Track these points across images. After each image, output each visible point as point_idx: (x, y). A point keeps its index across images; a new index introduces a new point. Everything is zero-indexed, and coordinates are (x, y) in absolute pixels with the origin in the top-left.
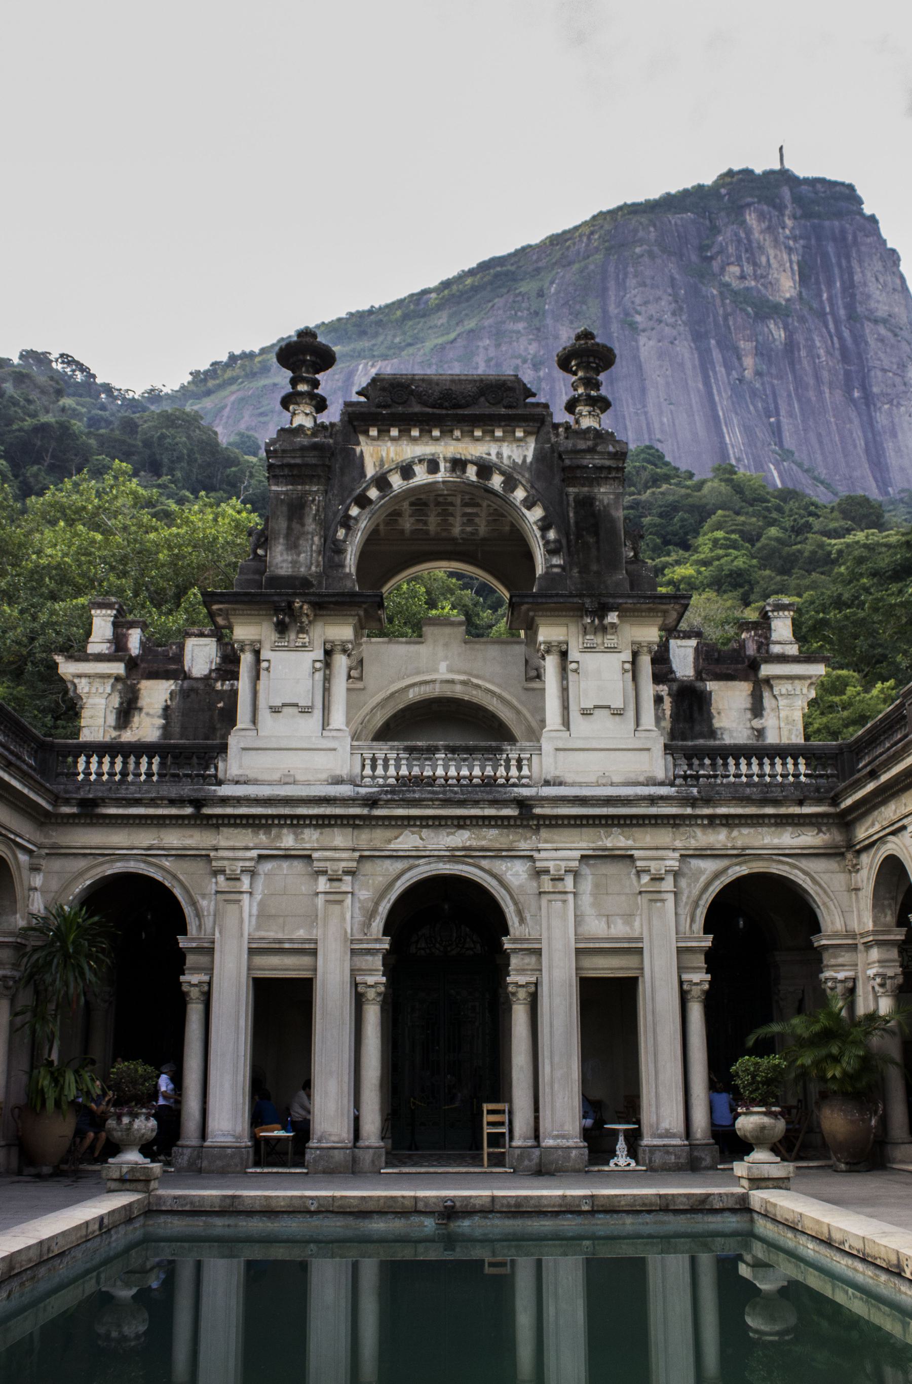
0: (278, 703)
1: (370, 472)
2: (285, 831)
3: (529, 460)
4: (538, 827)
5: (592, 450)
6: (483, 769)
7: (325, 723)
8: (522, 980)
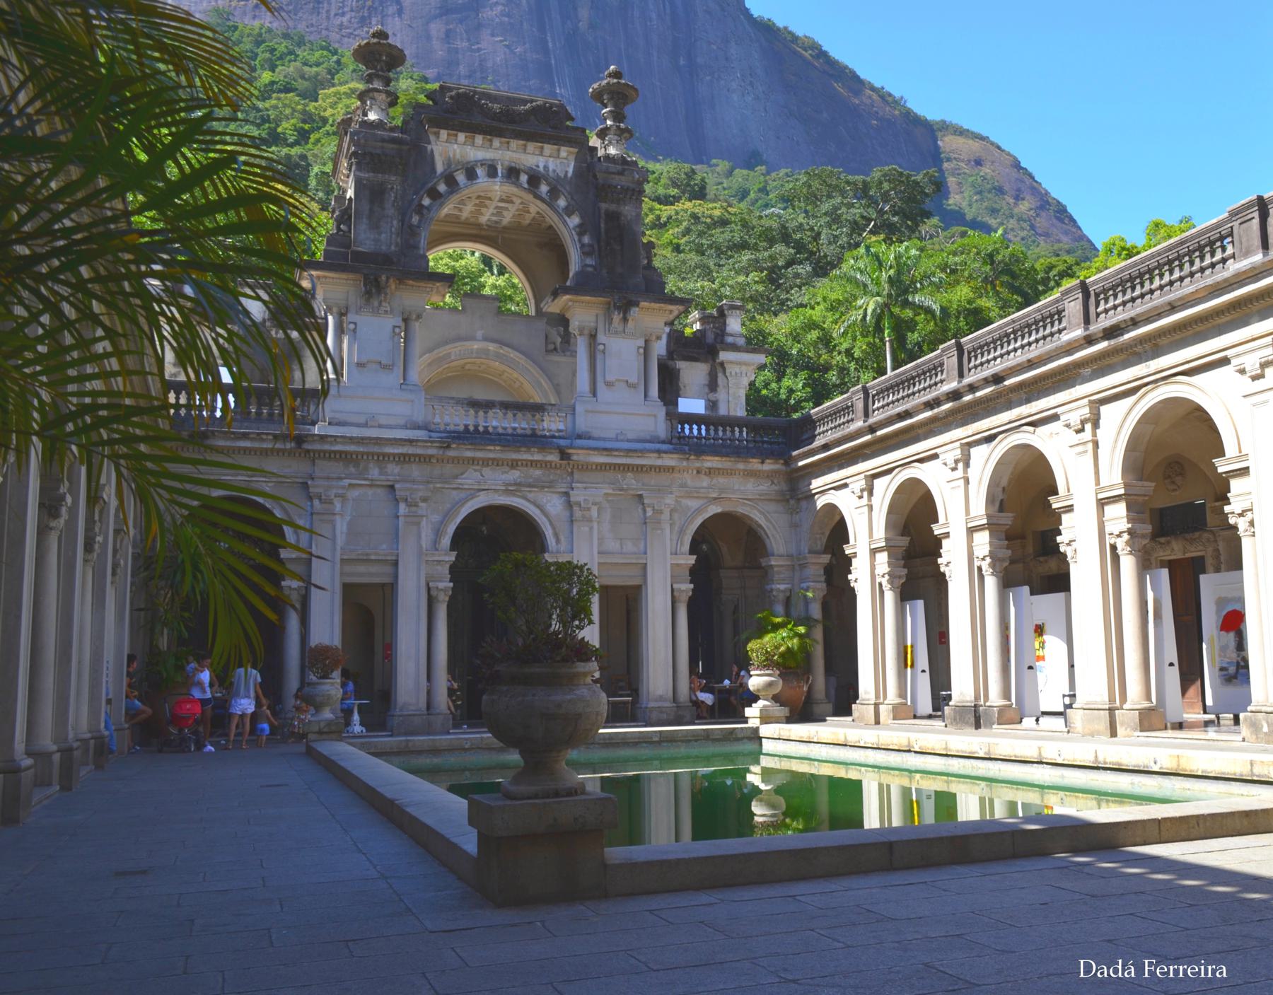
0: (364, 360)
1: (440, 168)
3: (570, 174)
5: (621, 173)
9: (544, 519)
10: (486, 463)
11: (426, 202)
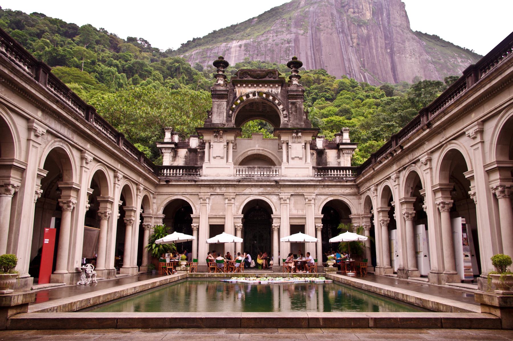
1: (238, 95)
4: (280, 187)
6: (267, 172)
7: (227, 161)
8: (276, 225)
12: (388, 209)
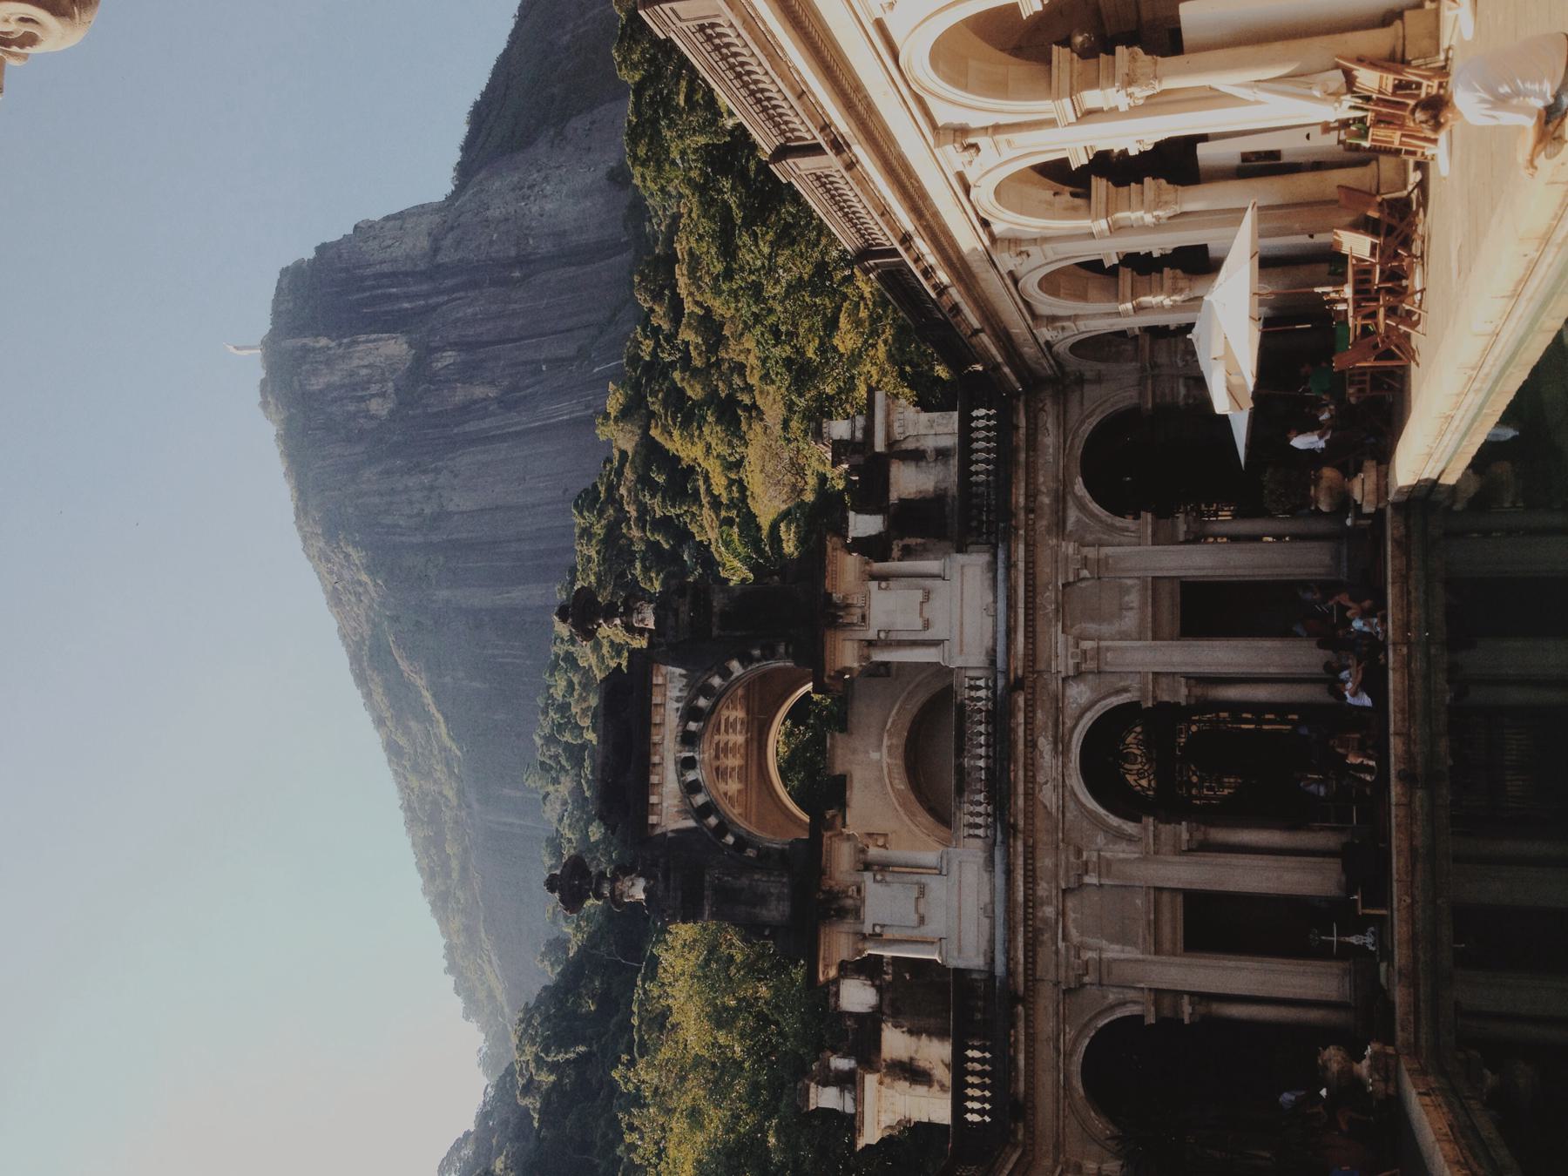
0: (915, 917)
1: (691, 823)
2: (1040, 914)
8: (1184, 691)
9: (1097, 707)
10: (1031, 779)
11: (730, 839)
12: (1126, 276)
